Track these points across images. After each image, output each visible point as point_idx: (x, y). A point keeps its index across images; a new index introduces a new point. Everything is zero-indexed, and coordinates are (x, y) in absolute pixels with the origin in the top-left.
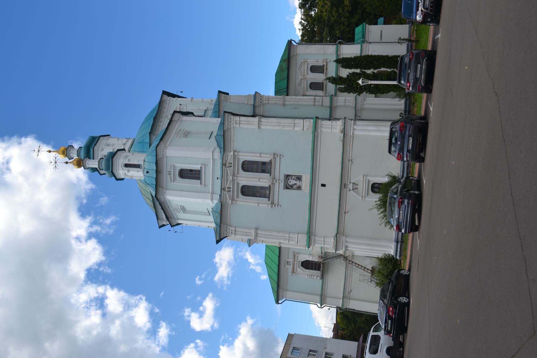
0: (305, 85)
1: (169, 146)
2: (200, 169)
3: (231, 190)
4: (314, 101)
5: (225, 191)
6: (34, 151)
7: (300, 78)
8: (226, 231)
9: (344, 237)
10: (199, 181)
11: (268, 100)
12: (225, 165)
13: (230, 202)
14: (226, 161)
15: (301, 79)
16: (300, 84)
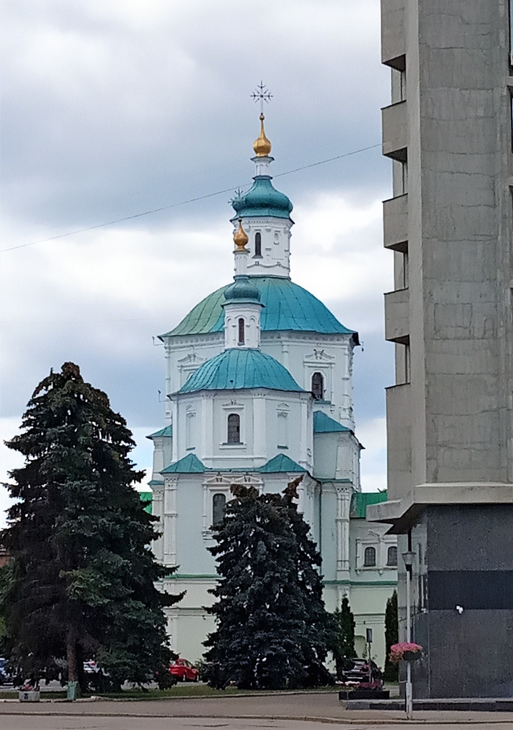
0: (371, 541)
1: (266, 399)
2: (241, 441)
3: (219, 483)
4: (343, 560)
5: (218, 475)
6: (262, 87)
7: (380, 534)
8: (171, 479)
9: (176, 617)
10: (226, 442)
11: (342, 500)
12: (247, 474)
13: (205, 482)
14: (251, 475)
15: (378, 535)
16: (371, 533)
